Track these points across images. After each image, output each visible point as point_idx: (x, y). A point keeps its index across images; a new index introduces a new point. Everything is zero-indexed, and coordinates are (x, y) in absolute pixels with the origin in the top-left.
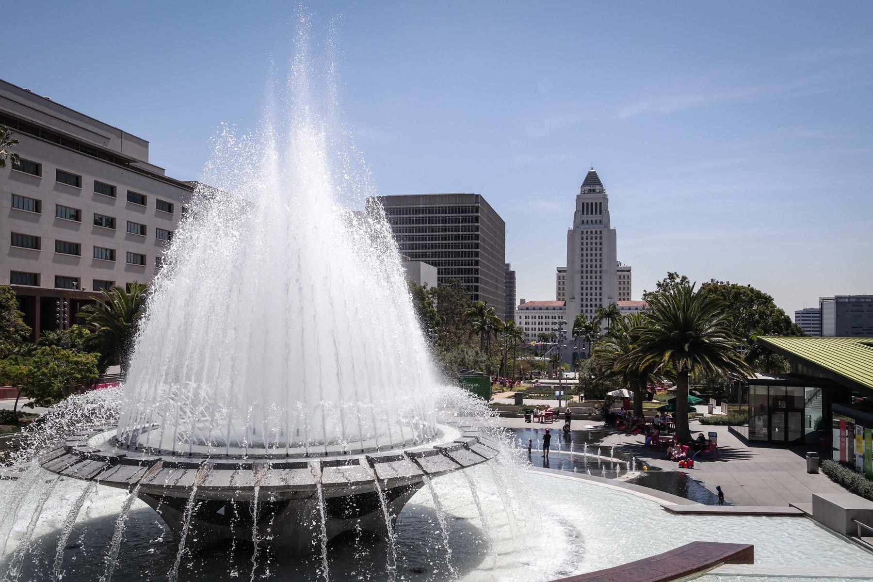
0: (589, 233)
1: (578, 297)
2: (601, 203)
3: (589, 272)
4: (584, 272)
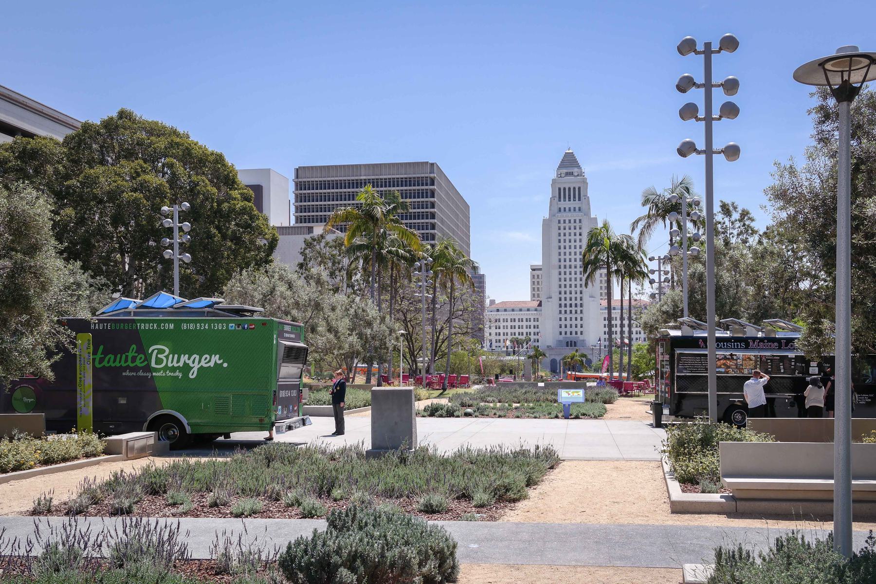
0: (567, 222)
1: (555, 296)
2: (579, 188)
3: (568, 267)
4: (562, 267)
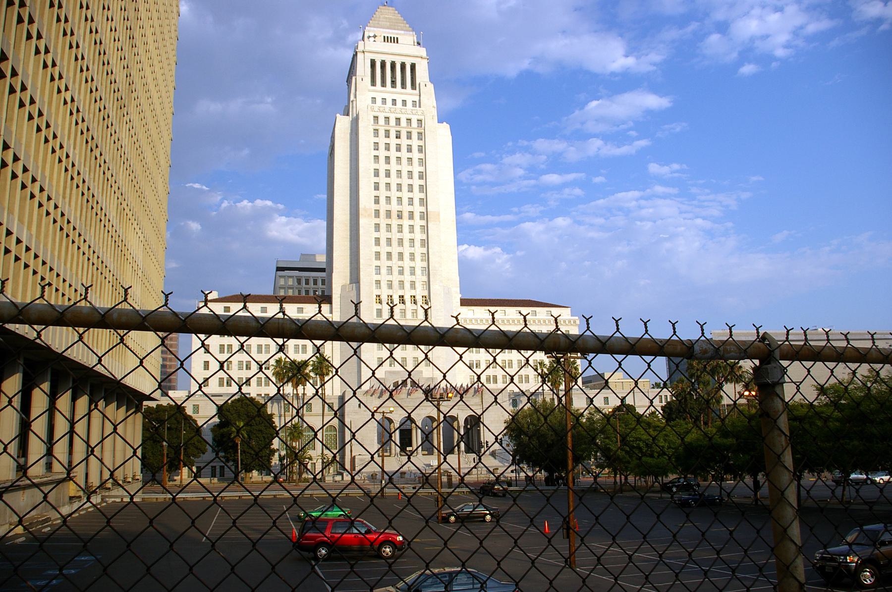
2: (413, 67)
3: (394, 215)
4: (383, 214)
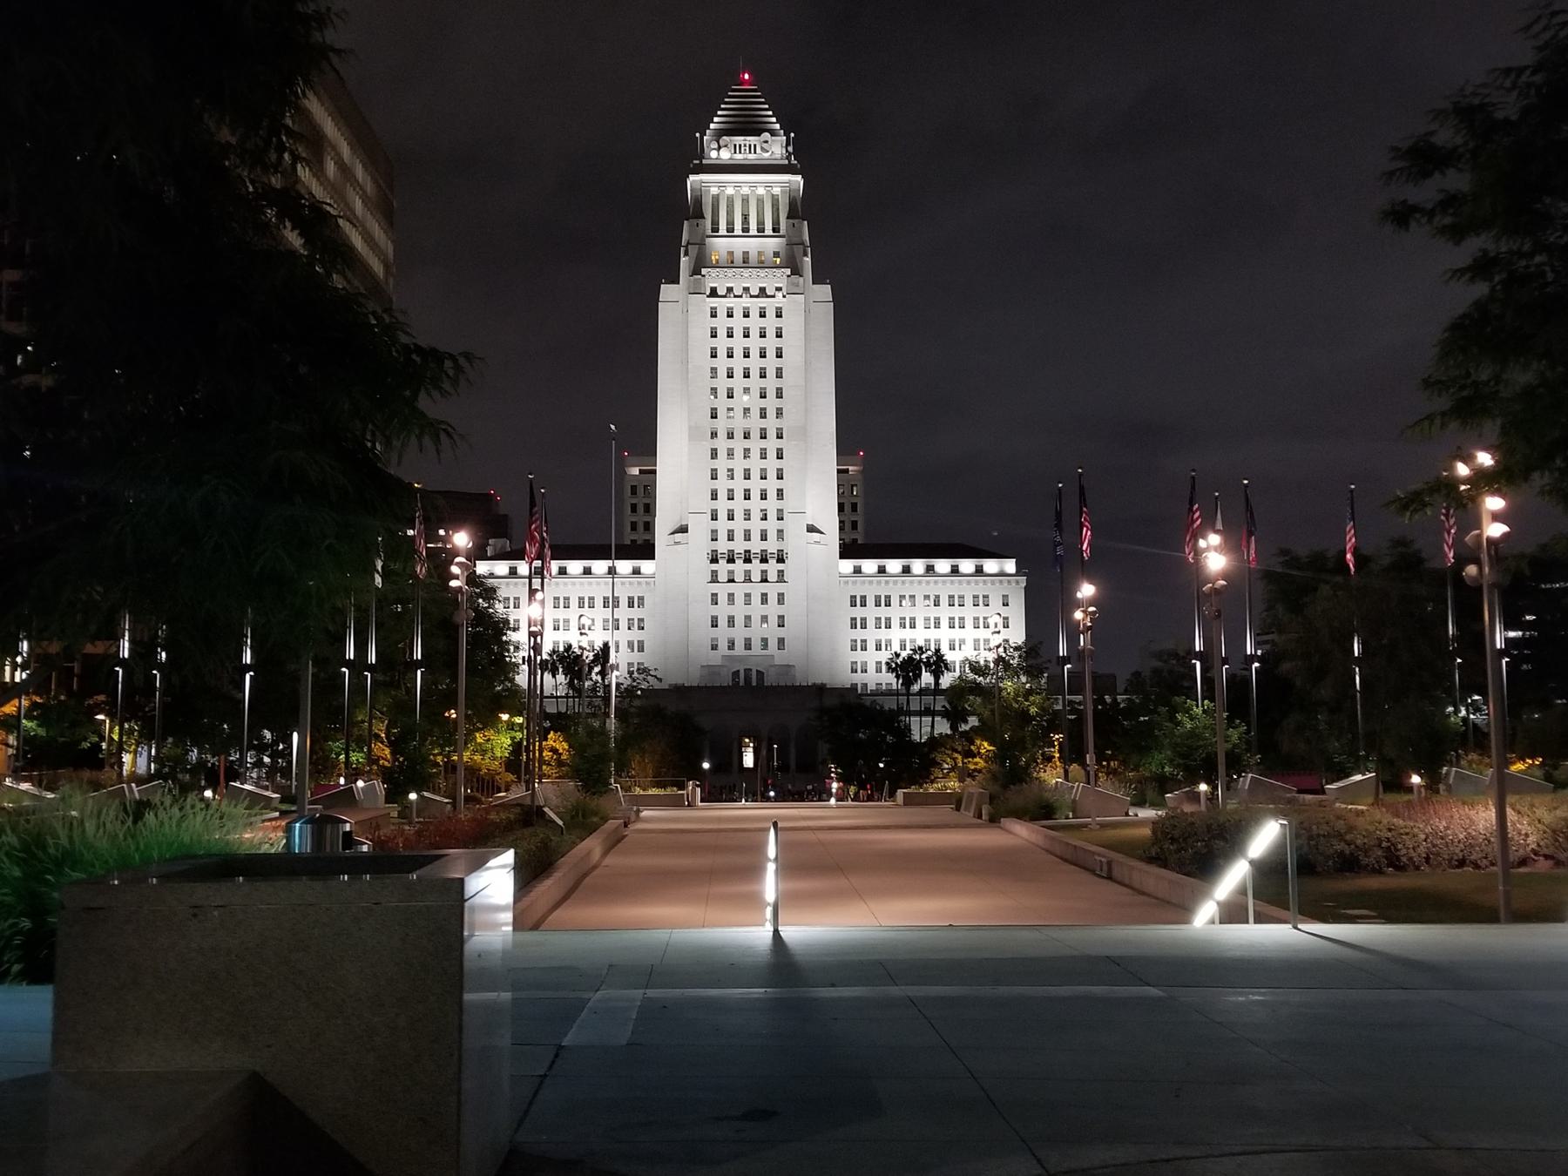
1: (700, 527)
